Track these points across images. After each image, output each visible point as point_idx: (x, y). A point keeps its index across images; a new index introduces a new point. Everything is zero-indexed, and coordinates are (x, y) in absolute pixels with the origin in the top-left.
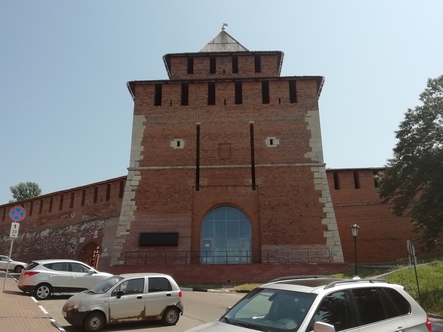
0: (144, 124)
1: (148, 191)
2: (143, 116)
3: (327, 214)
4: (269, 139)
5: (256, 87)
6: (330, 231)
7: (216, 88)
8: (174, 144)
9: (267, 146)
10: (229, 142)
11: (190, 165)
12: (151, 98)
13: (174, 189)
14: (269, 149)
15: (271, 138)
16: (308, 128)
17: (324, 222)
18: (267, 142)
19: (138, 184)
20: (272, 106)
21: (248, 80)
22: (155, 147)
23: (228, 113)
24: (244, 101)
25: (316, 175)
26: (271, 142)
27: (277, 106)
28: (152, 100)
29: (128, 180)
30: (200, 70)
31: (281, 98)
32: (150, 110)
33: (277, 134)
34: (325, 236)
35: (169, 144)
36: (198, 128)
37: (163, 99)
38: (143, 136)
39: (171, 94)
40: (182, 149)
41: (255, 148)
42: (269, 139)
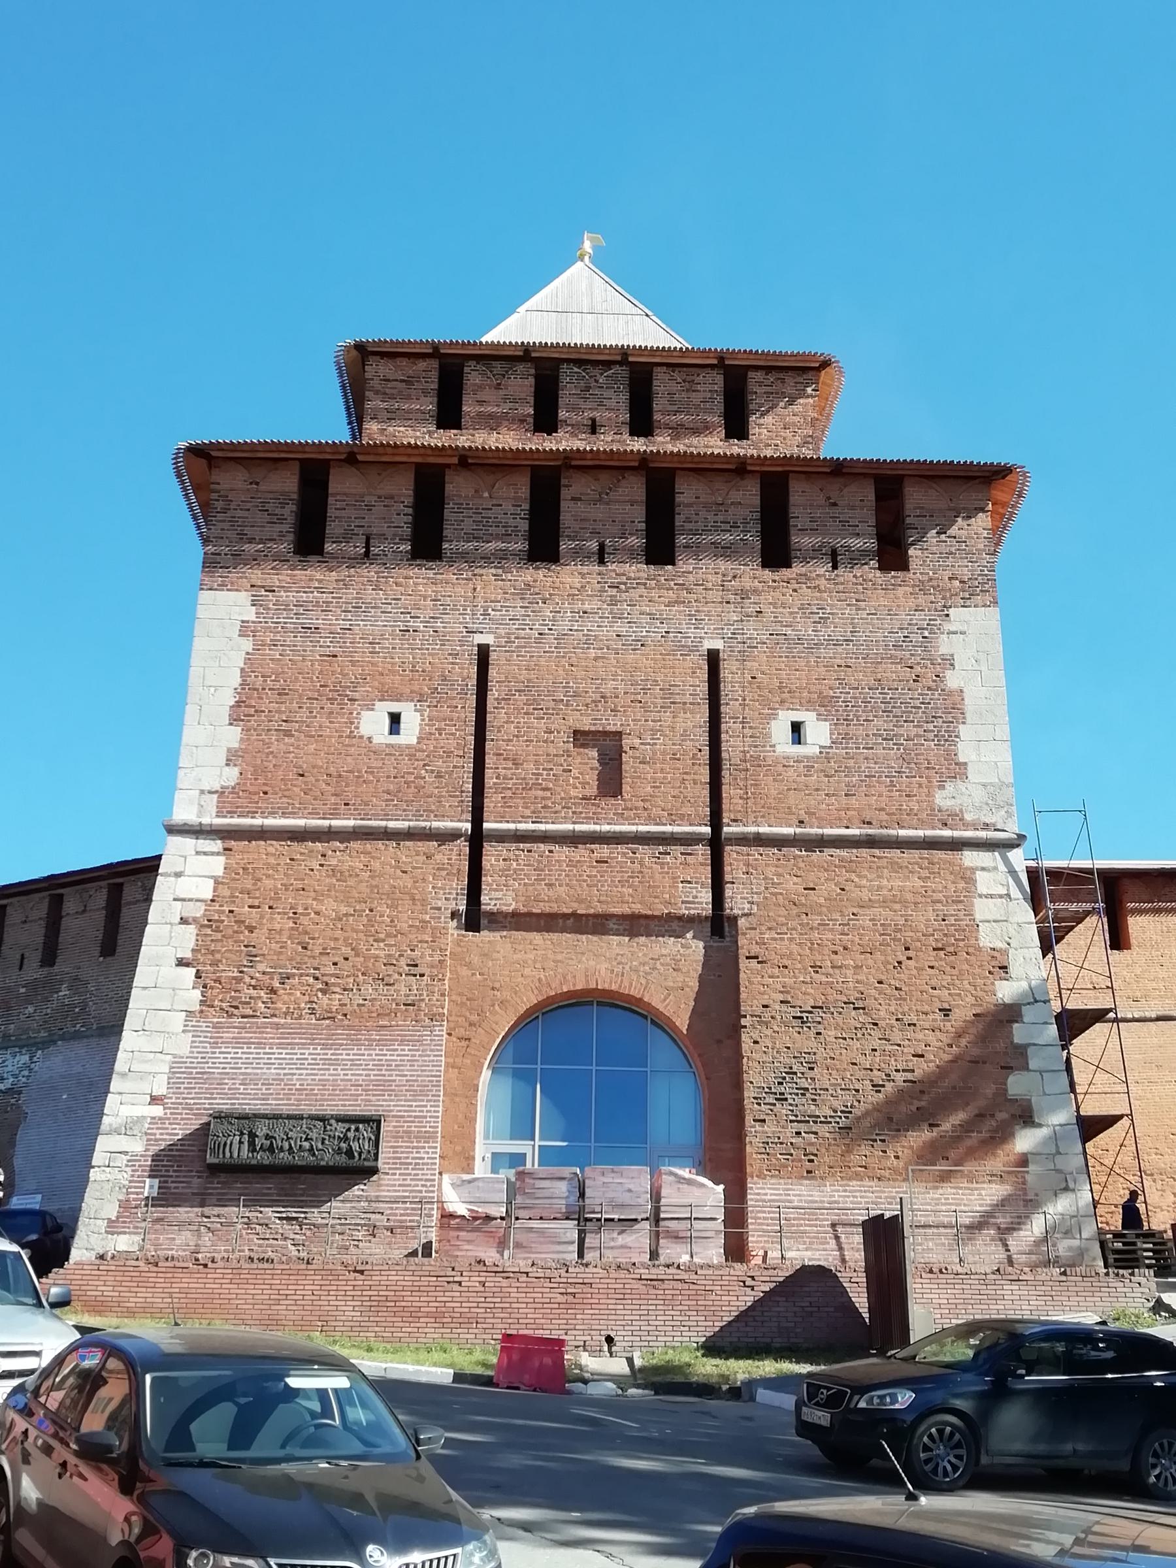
2: (244, 597)
3: (1030, 1050)
4: (786, 717)
5: (736, 496)
7: (565, 493)
8: (373, 724)
9: (779, 749)
12: (282, 520)
14: (785, 763)
15: (797, 716)
17: (1017, 1084)
18: (780, 730)
19: (209, 895)
21: (704, 468)
23: (614, 602)
27: (822, 582)
28: (285, 528)
29: (166, 875)
33: (823, 704)
36: (483, 654)
37: (333, 528)
38: (236, 680)
39: (369, 508)
40: (408, 747)
41: (724, 755)
42: (786, 717)
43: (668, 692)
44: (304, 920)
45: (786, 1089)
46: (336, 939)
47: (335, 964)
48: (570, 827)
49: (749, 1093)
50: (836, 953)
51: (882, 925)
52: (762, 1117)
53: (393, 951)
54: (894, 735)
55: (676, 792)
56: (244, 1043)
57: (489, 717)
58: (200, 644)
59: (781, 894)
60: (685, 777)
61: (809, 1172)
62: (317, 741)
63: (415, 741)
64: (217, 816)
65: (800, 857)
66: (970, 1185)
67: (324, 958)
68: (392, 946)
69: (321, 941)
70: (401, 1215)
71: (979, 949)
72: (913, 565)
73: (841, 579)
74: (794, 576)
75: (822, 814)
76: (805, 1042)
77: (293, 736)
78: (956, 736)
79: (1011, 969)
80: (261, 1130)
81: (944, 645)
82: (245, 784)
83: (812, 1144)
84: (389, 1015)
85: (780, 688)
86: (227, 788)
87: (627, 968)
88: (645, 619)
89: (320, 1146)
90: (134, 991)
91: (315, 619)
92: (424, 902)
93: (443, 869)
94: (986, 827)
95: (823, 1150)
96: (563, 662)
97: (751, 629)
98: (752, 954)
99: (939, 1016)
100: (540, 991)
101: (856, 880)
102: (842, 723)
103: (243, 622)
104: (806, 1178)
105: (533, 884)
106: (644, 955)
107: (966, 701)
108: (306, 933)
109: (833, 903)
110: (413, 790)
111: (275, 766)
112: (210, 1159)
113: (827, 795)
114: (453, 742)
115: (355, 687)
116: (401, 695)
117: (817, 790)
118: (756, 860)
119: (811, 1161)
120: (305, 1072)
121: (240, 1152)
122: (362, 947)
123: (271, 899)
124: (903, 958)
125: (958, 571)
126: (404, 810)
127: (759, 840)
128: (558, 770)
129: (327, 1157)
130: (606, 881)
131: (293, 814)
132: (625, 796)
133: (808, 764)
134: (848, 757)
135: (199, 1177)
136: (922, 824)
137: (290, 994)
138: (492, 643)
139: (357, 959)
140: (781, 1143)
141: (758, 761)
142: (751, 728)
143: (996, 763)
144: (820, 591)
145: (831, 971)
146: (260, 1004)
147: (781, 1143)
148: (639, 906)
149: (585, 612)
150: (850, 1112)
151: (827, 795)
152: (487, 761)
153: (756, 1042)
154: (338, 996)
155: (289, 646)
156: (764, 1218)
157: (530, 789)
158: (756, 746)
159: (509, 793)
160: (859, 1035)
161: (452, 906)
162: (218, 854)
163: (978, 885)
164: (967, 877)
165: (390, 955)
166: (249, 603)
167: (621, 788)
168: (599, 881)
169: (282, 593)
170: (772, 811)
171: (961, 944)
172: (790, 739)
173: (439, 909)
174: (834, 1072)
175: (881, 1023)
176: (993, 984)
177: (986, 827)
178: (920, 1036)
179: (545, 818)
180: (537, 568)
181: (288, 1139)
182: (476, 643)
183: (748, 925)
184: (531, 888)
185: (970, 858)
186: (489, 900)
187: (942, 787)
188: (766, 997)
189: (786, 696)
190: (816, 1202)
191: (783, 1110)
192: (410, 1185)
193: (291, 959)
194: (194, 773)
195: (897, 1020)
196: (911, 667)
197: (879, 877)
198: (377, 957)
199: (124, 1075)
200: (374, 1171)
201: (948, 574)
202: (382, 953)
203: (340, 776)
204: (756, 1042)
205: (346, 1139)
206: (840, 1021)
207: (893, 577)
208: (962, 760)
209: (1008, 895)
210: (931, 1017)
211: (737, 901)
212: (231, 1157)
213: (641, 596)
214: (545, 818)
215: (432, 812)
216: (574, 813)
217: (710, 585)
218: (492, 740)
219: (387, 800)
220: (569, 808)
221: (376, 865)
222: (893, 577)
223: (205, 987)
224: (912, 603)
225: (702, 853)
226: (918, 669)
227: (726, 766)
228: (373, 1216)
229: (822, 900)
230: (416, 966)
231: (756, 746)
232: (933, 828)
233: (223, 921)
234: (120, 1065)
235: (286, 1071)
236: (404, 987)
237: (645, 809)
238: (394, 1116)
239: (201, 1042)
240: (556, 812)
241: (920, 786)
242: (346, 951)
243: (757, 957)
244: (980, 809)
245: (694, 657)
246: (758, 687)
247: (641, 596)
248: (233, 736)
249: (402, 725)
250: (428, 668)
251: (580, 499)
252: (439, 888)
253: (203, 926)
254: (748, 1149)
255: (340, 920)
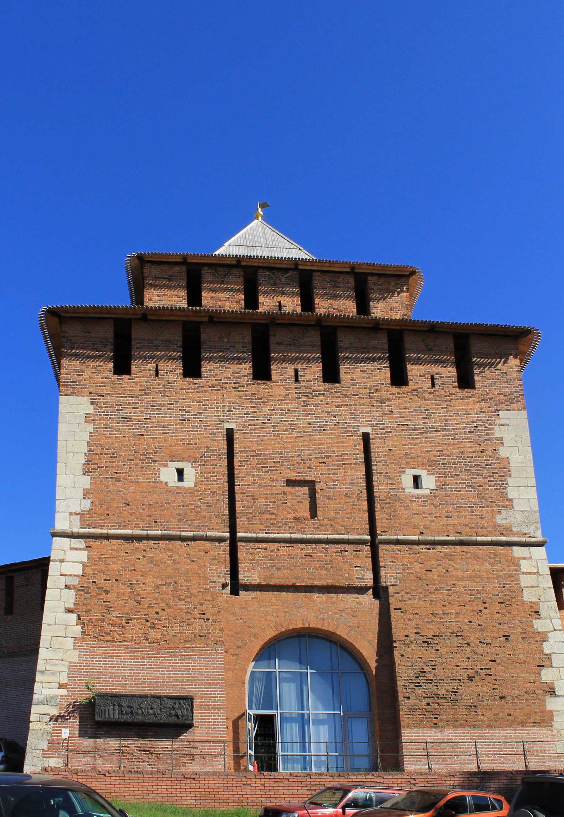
1: (107, 592)
3: (553, 657)
6: (559, 696)
7: (272, 340)
9: (407, 491)
11: (213, 529)
13: (175, 590)
15: (417, 472)
16: (503, 452)
20: (416, 392)
22: (118, 480)
23: (306, 405)
25: (525, 566)
26: (416, 480)
27: (426, 395)
29: (55, 561)
31: (436, 376)
32: (104, 385)
33: (431, 465)
34: (549, 707)
35: (156, 474)
36: (230, 434)
38: (86, 449)
40: (190, 488)
41: (375, 494)
43: (341, 456)
44: (137, 588)
45: (421, 680)
46: (156, 599)
47: (157, 613)
48: (289, 535)
49: (400, 683)
50: (444, 606)
51: (470, 590)
52: (408, 696)
53: (190, 605)
54: (472, 483)
55: (349, 516)
56: (109, 656)
57: (236, 472)
58: (62, 427)
59: (412, 573)
60: (354, 507)
61: (435, 724)
62: (135, 485)
63: (193, 485)
64: (81, 528)
65: (422, 552)
66: (523, 729)
67: (150, 609)
68: (189, 603)
69: (147, 599)
70: (208, 749)
71: (523, 602)
72: (477, 386)
73: (437, 393)
74: (410, 390)
75: (433, 528)
76: (430, 654)
77: (121, 481)
78: (507, 484)
79: (541, 613)
80: (125, 703)
81: (498, 432)
82: (95, 509)
83: (436, 709)
84: (191, 641)
85: (405, 456)
86: (85, 511)
87: (326, 615)
88: (324, 415)
89: (159, 712)
90: (43, 626)
91: (130, 412)
92: (205, 578)
93: (216, 559)
94: (524, 535)
95: (443, 712)
96: (278, 439)
97: (387, 421)
98: (398, 607)
99: (503, 639)
100: (277, 629)
101: (454, 565)
102: (441, 476)
103: (87, 414)
104: (434, 727)
105: (268, 568)
106: (335, 608)
107: (511, 464)
108: (139, 595)
109: (442, 578)
110: (194, 514)
111: (112, 499)
112: (97, 719)
113: (435, 517)
114: (215, 486)
115: (155, 452)
116: (183, 458)
117: (430, 514)
118: (397, 554)
119: (436, 718)
120: (145, 672)
121: (114, 715)
122: (172, 603)
123: (116, 575)
124: (482, 608)
125: (503, 390)
126: (190, 526)
127: (398, 542)
128: (279, 503)
129: (164, 718)
130: (311, 566)
131: (125, 527)
132: (319, 518)
133: (424, 499)
134: (447, 496)
135: (91, 728)
136: (489, 534)
137: (132, 629)
138: (235, 428)
139: (170, 610)
140: (420, 709)
141: (395, 499)
142: (390, 478)
143: (528, 499)
144: (425, 400)
145: (442, 616)
146: (116, 635)
147: (420, 709)
148: (331, 581)
149: (289, 410)
150: (457, 692)
151: (435, 517)
152: (236, 497)
153: (402, 656)
154: (160, 631)
155: (115, 429)
156: (412, 749)
157: (263, 513)
158: (393, 489)
159: (251, 516)
160: (460, 651)
161: (223, 580)
162: (83, 549)
163: (522, 567)
164: (515, 563)
165: (188, 608)
166: (89, 403)
167: (317, 513)
168: (307, 567)
169: (109, 398)
170: (404, 527)
171: (514, 600)
172: (412, 486)
173: (215, 582)
174: (447, 671)
175: (472, 644)
176: (532, 621)
177: (524, 535)
178: (494, 650)
179: (273, 530)
180: (259, 384)
181: (141, 708)
182: (225, 428)
183: (394, 591)
184: (267, 571)
185: (517, 551)
186: (243, 577)
187: (500, 513)
188: (407, 631)
189: (409, 460)
190: (440, 739)
191: (419, 691)
192: (212, 733)
193: (132, 609)
194: (65, 503)
195: (480, 642)
196: (480, 444)
197: (467, 563)
198: (180, 609)
199: (42, 672)
200: (191, 726)
201: (497, 391)
202: (183, 607)
203: (150, 505)
204: (402, 656)
205: (174, 709)
206: (449, 642)
207: (467, 392)
208: (510, 497)
209: (538, 572)
210: (499, 639)
211: (388, 577)
212: (109, 717)
213: (322, 401)
214: (273, 530)
215: (206, 526)
216: (290, 527)
217: (361, 395)
218: (239, 485)
219: (179, 519)
220: (286, 525)
221: (176, 557)
222: (467, 392)
223: (83, 624)
224: (478, 407)
225: (366, 550)
226: (483, 445)
227: (377, 500)
228: (192, 750)
229: (436, 577)
230: (204, 614)
231: (393, 489)
232: (495, 536)
233: (90, 587)
234: (41, 665)
235: (135, 672)
236: (198, 626)
237: (332, 525)
238: (199, 697)
239: (84, 655)
240: (279, 527)
241: (487, 512)
242: (163, 605)
243: (400, 609)
244: (520, 525)
245: (355, 437)
246: (393, 455)
247: (322, 401)
248: (85, 481)
249: (185, 476)
250: (198, 442)
251: (281, 344)
252: (215, 570)
253: (78, 590)
254: (401, 713)
255: (158, 587)
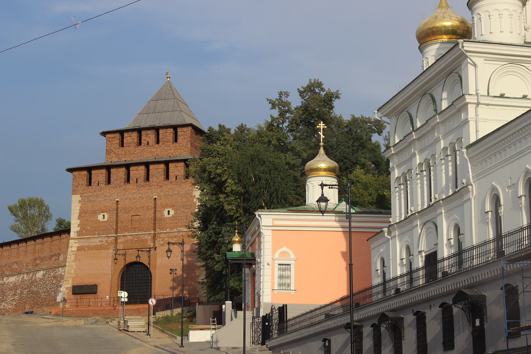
0: (80, 202)
4: (167, 210)
8: (100, 217)
10: (139, 214)
15: (169, 209)
18: (166, 212)
24: (150, 179)
30: (129, 143)
33: (172, 206)
35: (97, 217)
38: (79, 212)
42: (167, 210)
58: (73, 205)
189: (167, 206)
